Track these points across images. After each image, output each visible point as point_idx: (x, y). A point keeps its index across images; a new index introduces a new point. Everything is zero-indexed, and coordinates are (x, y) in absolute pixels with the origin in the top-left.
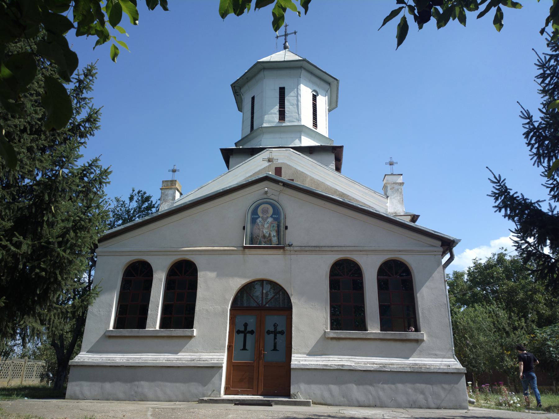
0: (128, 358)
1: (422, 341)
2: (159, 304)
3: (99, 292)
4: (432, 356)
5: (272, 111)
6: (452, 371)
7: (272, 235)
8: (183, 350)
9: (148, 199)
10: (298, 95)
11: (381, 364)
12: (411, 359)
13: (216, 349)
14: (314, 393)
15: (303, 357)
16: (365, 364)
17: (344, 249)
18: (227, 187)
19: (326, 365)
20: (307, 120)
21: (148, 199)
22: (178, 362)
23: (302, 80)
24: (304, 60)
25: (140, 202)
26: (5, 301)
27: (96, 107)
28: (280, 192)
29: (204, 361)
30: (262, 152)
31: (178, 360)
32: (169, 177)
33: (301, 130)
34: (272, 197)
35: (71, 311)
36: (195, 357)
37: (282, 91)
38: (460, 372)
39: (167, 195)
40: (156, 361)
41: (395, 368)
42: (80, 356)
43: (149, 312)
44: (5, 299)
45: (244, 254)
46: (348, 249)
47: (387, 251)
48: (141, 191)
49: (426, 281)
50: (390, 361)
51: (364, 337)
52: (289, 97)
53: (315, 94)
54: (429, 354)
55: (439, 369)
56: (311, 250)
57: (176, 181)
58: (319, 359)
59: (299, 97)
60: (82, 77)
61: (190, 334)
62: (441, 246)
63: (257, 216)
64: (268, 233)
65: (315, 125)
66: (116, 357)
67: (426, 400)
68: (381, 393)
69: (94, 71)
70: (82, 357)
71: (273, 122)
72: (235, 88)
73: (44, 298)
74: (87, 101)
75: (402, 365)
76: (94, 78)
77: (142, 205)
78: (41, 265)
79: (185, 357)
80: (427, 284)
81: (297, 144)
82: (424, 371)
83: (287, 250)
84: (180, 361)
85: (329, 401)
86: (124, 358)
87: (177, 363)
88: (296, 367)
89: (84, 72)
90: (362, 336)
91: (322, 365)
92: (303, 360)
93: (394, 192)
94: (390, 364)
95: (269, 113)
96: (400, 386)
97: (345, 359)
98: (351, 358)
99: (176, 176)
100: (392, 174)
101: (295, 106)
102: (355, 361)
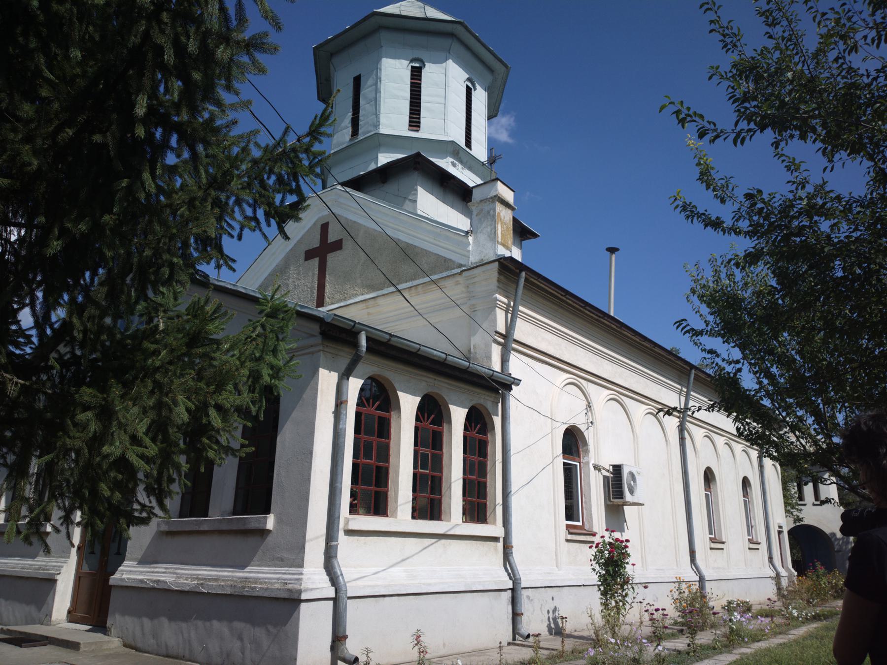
5: (343, 125)
14: (127, 628)
19: (142, 581)
41: (212, 588)
51: (196, 528)
52: (367, 88)
53: (417, 65)
58: (145, 570)
59: (379, 83)
65: (415, 122)
71: (343, 144)
75: (229, 580)
82: (246, 594)
93: (483, 219)
101: (373, 103)
102: (178, 574)
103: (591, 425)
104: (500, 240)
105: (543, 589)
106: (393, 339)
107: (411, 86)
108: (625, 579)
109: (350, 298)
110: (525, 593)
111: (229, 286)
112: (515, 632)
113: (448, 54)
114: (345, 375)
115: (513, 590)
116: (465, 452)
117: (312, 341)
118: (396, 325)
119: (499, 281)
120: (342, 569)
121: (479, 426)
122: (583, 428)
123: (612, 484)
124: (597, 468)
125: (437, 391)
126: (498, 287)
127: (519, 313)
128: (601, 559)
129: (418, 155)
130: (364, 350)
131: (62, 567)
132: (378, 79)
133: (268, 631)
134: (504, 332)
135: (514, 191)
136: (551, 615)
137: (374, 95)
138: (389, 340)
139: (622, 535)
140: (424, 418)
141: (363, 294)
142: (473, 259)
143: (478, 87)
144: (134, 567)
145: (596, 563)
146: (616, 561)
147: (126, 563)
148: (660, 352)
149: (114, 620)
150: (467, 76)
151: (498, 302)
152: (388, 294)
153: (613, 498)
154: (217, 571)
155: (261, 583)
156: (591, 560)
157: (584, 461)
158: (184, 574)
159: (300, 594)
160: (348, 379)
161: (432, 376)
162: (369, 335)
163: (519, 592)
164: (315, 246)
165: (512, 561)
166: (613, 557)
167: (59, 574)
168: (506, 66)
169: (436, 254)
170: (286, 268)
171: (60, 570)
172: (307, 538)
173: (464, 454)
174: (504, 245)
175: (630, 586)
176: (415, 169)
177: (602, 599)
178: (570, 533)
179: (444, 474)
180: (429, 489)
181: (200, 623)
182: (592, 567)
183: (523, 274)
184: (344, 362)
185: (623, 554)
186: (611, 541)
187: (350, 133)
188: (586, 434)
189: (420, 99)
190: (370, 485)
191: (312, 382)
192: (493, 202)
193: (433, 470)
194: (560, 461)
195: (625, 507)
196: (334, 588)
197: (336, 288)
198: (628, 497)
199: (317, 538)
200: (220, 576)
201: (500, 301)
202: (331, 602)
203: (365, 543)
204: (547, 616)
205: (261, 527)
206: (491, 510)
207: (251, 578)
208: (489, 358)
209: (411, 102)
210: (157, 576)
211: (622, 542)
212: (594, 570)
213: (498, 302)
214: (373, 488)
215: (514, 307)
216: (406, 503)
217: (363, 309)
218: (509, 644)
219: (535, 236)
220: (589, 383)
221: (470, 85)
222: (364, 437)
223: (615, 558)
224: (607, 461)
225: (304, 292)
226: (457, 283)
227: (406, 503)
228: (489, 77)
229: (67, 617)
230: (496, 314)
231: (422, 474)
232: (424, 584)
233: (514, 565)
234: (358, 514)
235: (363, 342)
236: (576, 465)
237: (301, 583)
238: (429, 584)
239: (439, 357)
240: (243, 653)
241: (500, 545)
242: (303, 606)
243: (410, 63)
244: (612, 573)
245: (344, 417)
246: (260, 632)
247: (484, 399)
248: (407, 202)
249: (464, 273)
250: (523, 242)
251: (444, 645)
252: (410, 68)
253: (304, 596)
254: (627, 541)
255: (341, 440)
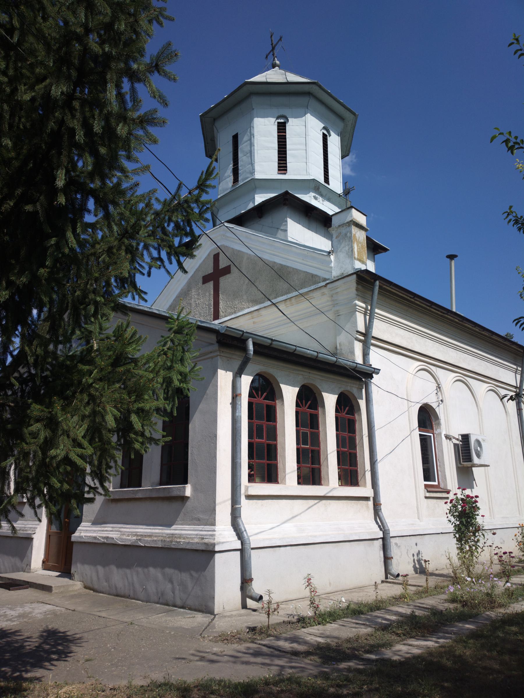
5: (226, 175)
14: (86, 574)
19: (95, 538)
41: (147, 542)
53: (282, 121)
58: (97, 529)
59: (252, 138)
65: (282, 167)
68: (135, 578)
71: (227, 189)
75: (159, 536)
82: (173, 547)
85: (96, 587)
93: (341, 241)
95: (224, 178)
101: (249, 155)
103: (441, 403)
104: (356, 256)
105: (408, 537)
106: (274, 343)
107: (278, 138)
108: (477, 527)
109: (239, 311)
110: (393, 541)
111: (146, 309)
112: (387, 572)
113: (306, 109)
114: (238, 374)
115: (383, 539)
116: (337, 430)
117: (211, 348)
118: (276, 331)
119: (357, 290)
120: (245, 526)
121: (347, 408)
122: (434, 406)
123: (462, 450)
124: (448, 437)
125: (312, 382)
126: (357, 295)
127: (375, 315)
128: (456, 512)
129: (287, 193)
130: (252, 353)
131: (36, 528)
132: (252, 135)
133: (191, 575)
134: (364, 331)
135: (366, 216)
136: (416, 558)
137: (249, 149)
138: (271, 344)
139: (472, 491)
140: (302, 404)
141: (249, 308)
142: (335, 273)
143: (332, 133)
144: (89, 527)
145: (451, 516)
146: (468, 513)
147: (83, 524)
148: (497, 339)
149: (76, 568)
150: (323, 125)
151: (357, 307)
152: (268, 306)
153: (463, 462)
154: (150, 529)
155: (184, 539)
156: (447, 514)
157: (437, 432)
158: (126, 532)
159: (214, 547)
160: (241, 377)
161: (307, 371)
162: (255, 341)
163: (388, 541)
164: (210, 272)
165: (381, 516)
166: (465, 510)
167: (35, 533)
168: (354, 114)
169: (305, 272)
170: (189, 291)
171: (35, 531)
172: (217, 502)
173: (336, 431)
174: (360, 260)
175: (480, 534)
176: (285, 204)
177: (457, 544)
178: (428, 492)
179: (321, 448)
180: (310, 460)
181: (140, 570)
182: (448, 519)
183: (377, 283)
184: (237, 364)
185: (474, 507)
186: (463, 497)
187: (232, 181)
188: (437, 410)
189: (286, 148)
190: (263, 459)
191: (213, 380)
192: (349, 226)
193: (312, 445)
194: (417, 433)
195: (474, 469)
196: (240, 541)
197: (227, 304)
198: (476, 460)
199: (224, 502)
200: (153, 533)
201: (359, 306)
202: (239, 552)
203: (262, 505)
204: (412, 558)
205: (182, 495)
206: (362, 476)
207: (176, 534)
208: (353, 353)
209: (279, 151)
210: (106, 533)
211: (472, 497)
212: (450, 521)
213: (357, 307)
214: (265, 461)
215: (370, 310)
216: (292, 472)
217: (249, 319)
218: (383, 582)
219: (385, 250)
220: (437, 368)
221: (326, 132)
222: (256, 421)
223: (467, 511)
224: (457, 431)
225: (203, 308)
226: (323, 294)
227: (292, 472)
228: (341, 125)
229: (42, 565)
230: (356, 317)
231: (304, 449)
232: (311, 536)
233: (383, 519)
234: (255, 483)
235: (251, 347)
236: (431, 436)
237: (215, 538)
238: (315, 536)
239: (312, 355)
240: (173, 593)
241: (371, 503)
242: (217, 556)
243: (276, 120)
244: (465, 523)
245: (240, 407)
246: (185, 576)
247: (350, 386)
248: (280, 231)
249: (328, 286)
250: (376, 256)
251: (330, 584)
252: (276, 123)
253: (217, 549)
254: (477, 497)
255: (238, 425)
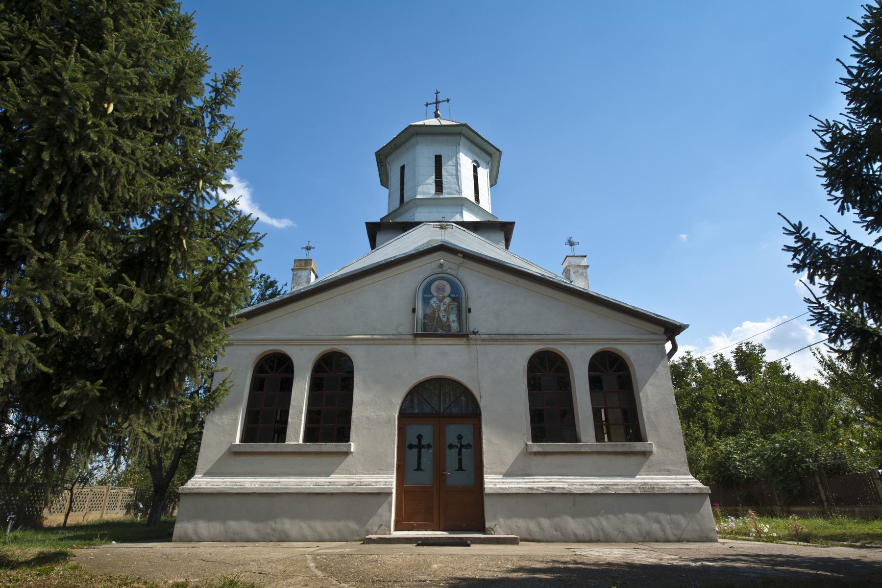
0: (261, 482)
1: (650, 453)
2: (302, 410)
3: (229, 388)
4: (663, 472)
5: (427, 182)
6: (693, 492)
7: (451, 320)
8: (337, 471)
9: (273, 284)
10: (457, 165)
11: (602, 485)
12: (638, 477)
13: (380, 469)
14: (516, 526)
15: (499, 479)
16: (581, 485)
17: (545, 337)
18: (391, 258)
19: (532, 489)
20: (468, 193)
21: (273, 284)
22: (330, 487)
23: (461, 148)
24: (465, 125)
25: (263, 288)
26: (100, 388)
27: (239, 128)
28: (460, 265)
29: (366, 485)
30: (418, 226)
31: (331, 485)
32: (303, 255)
33: (462, 203)
34: (449, 271)
35: (190, 415)
36: (354, 480)
37: (438, 160)
38: (702, 492)
39: (299, 277)
40: (301, 485)
41: (620, 489)
42: (194, 480)
43: (290, 420)
44: (102, 385)
45: (415, 344)
46: (551, 337)
47: (599, 340)
48: (264, 275)
49: (650, 377)
50: (613, 481)
53: (475, 164)
54: (660, 471)
55: (676, 488)
56: (504, 339)
57: (311, 260)
60: (220, 86)
61: (345, 450)
62: (664, 333)
63: (430, 296)
64: (446, 317)
66: (245, 482)
67: (663, 530)
69: (236, 80)
70: (198, 481)
71: (428, 194)
72: (381, 156)
73: (165, 385)
74: (225, 120)
76: (236, 90)
77: (266, 291)
78: (166, 328)
79: (339, 480)
80: (651, 380)
81: (458, 218)
82: (657, 492)
83: (472, 339)
84: (333, 485)
85: (538, 536)
86: (257, 482)
87: (330, 488)
88: (492, 491)
89: (223, 78)
90: (574, 450)
91: (526, 488)
92: (499, 482)
94: (613, 485)
95: (424, 183)
96: (629, 516)
97: (555, 480)
98: (562, 479)
99: (311, 255)
100: (574, 256)
181: (611, 516)
